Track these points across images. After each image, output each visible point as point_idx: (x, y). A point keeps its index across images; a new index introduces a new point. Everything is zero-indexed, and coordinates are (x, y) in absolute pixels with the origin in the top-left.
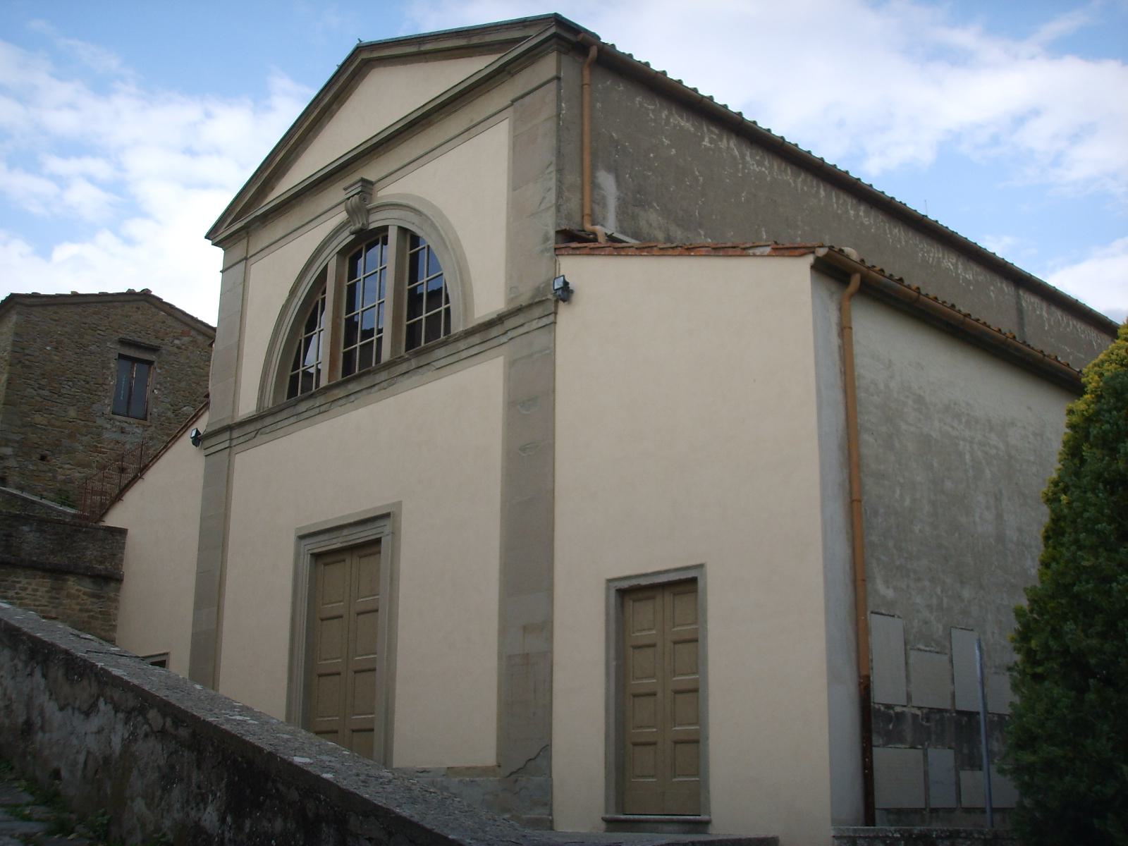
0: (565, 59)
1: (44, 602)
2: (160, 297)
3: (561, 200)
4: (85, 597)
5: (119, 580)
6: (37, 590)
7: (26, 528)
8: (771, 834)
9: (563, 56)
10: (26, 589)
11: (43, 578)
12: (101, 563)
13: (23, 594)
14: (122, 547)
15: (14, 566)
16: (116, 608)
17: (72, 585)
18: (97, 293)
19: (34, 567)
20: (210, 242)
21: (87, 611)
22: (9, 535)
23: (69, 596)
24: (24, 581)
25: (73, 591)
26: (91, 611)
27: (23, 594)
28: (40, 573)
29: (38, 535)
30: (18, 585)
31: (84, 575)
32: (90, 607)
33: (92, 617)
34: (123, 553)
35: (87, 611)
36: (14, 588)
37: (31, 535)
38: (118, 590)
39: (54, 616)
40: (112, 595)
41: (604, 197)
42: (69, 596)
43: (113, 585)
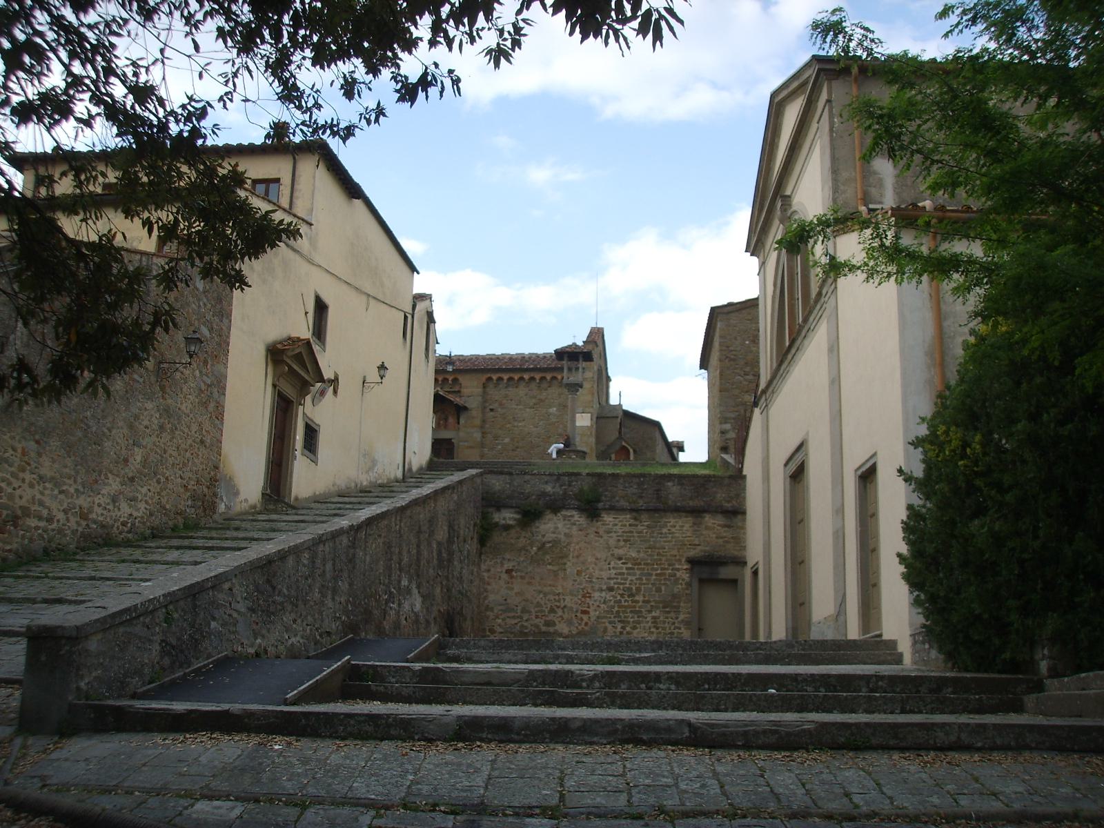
0: (834, 83)
1: (688, 535)
2: (461, 354)
3: (837, 194)
4: (719, 528)
5: (744, 513)
6: (683, 526)
7: (670, 484)
8: (893, 638)
9: (833, 82)
10: (675, 526)
11: (686, 517)
12: (729, 502)
13: (673, 530)
14: (744, 489)
15: (665, 511)
16: (745, 534)
17: (708, 520)
18: (726, 303)
19: (677, 510)
20: (749, 254)
21: (722, 538)
22: (658, 490)
23: (707, 528)
24: (673, 521)
25: (710, 524)
26: (725, 537)
27: (673, 530)
28: (684, 514)
29: (679, 487)
30: (669, 524)
31: (716, 512)
32: (725, 534)
33: (727, 542)
34: (745, 493)
35: (722, 538)
36: (666, 526)
37: (675, 488)
38: (744, 520)
39: (697, 543)
40: (740, 524)
41: (881, 180)
42: (707, 528)
43: (739, 517)
